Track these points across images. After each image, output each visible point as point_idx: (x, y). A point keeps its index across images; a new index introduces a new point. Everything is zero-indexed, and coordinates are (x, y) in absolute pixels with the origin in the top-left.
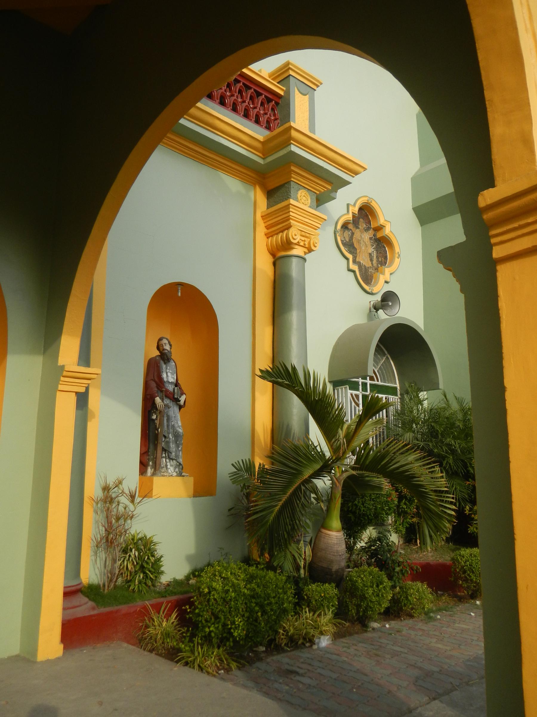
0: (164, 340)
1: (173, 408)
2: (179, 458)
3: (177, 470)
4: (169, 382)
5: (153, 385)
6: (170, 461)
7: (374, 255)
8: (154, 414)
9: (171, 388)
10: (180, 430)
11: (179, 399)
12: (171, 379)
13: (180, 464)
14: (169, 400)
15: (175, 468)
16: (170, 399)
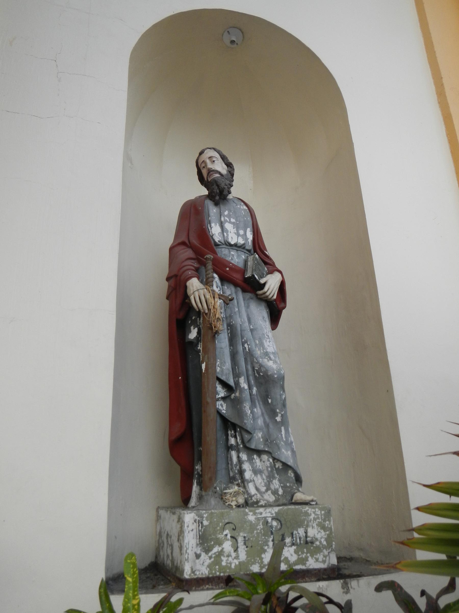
1: (248, 307)
2: (279, 449)
3: (276, 484)
4: (231, 245)
6: (250, 460)
8: (192, 328)
11: (258, 282)
12: (235, 237)
13: (286, 466)
14: (233, 288)
15: (270, 478)
16: (236, 285)
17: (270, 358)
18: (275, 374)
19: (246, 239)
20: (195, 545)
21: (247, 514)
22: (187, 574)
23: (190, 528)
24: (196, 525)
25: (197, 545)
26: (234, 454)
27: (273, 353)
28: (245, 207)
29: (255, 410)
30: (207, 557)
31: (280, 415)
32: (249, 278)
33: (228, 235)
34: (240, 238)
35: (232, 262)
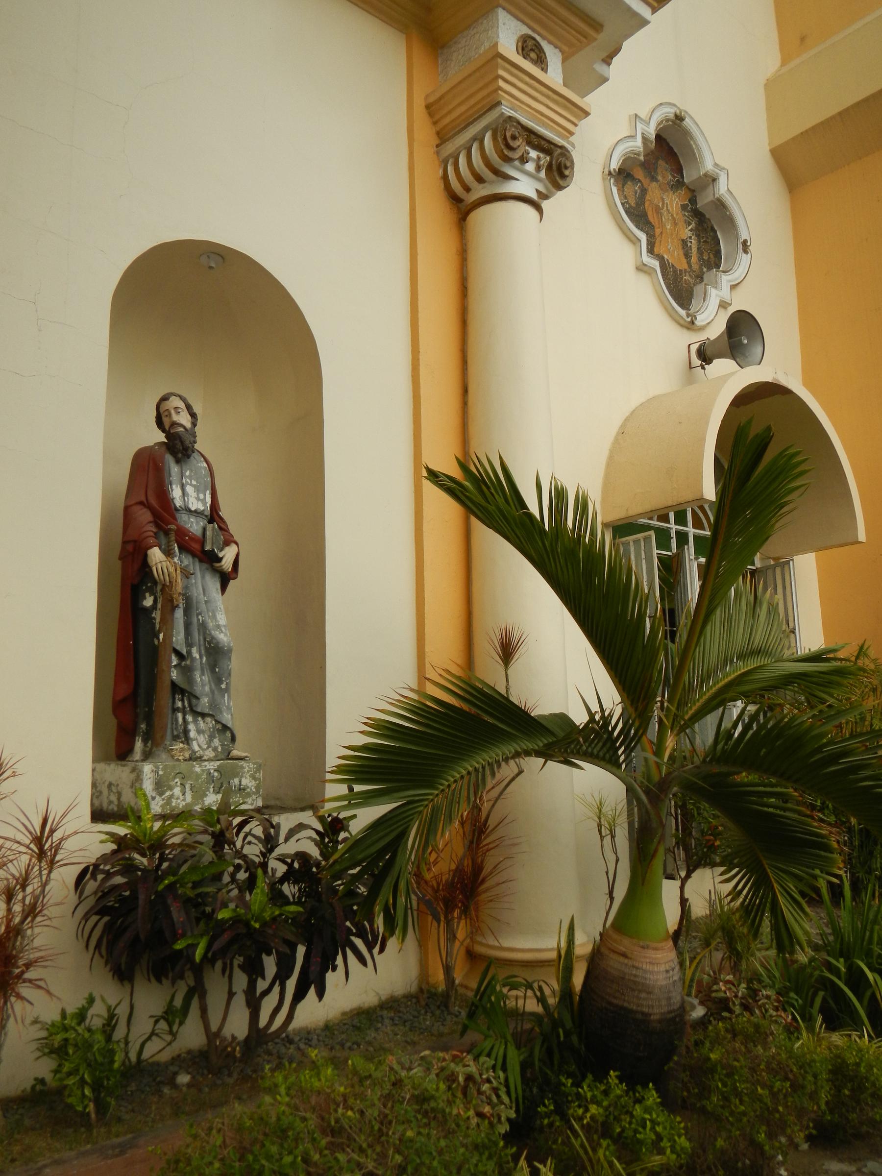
0: (173, 398)
1: (203, 577)
2: (221, 712)
3: (216, 742)
4: (190, 511)
5: (144, 516)
6: (195, 721)
7: (693, 246)
8: (147, 595)
9: (195, 526)
10: (223, 638)
11: (216, 556)
12: (195, 501)
13: (225, 728)
14: (191, 559)
15: (211, 738)
16: (194, 555)
17: (221, 630)
18: (225, 646)
19: (205, 503)
20: (151, 790)
21: (194, 766)
23: (148, 777)
24: (153, 774)
25: (153, 790)
26: (180, 716)
27: (224, 626)
28: (205, 465)
29: (204, 678)
30: (160, 799)
31: (225, 683)
32: (208, 551)
33: (188, 499)
34: (200, 502)
35: (191, 530)
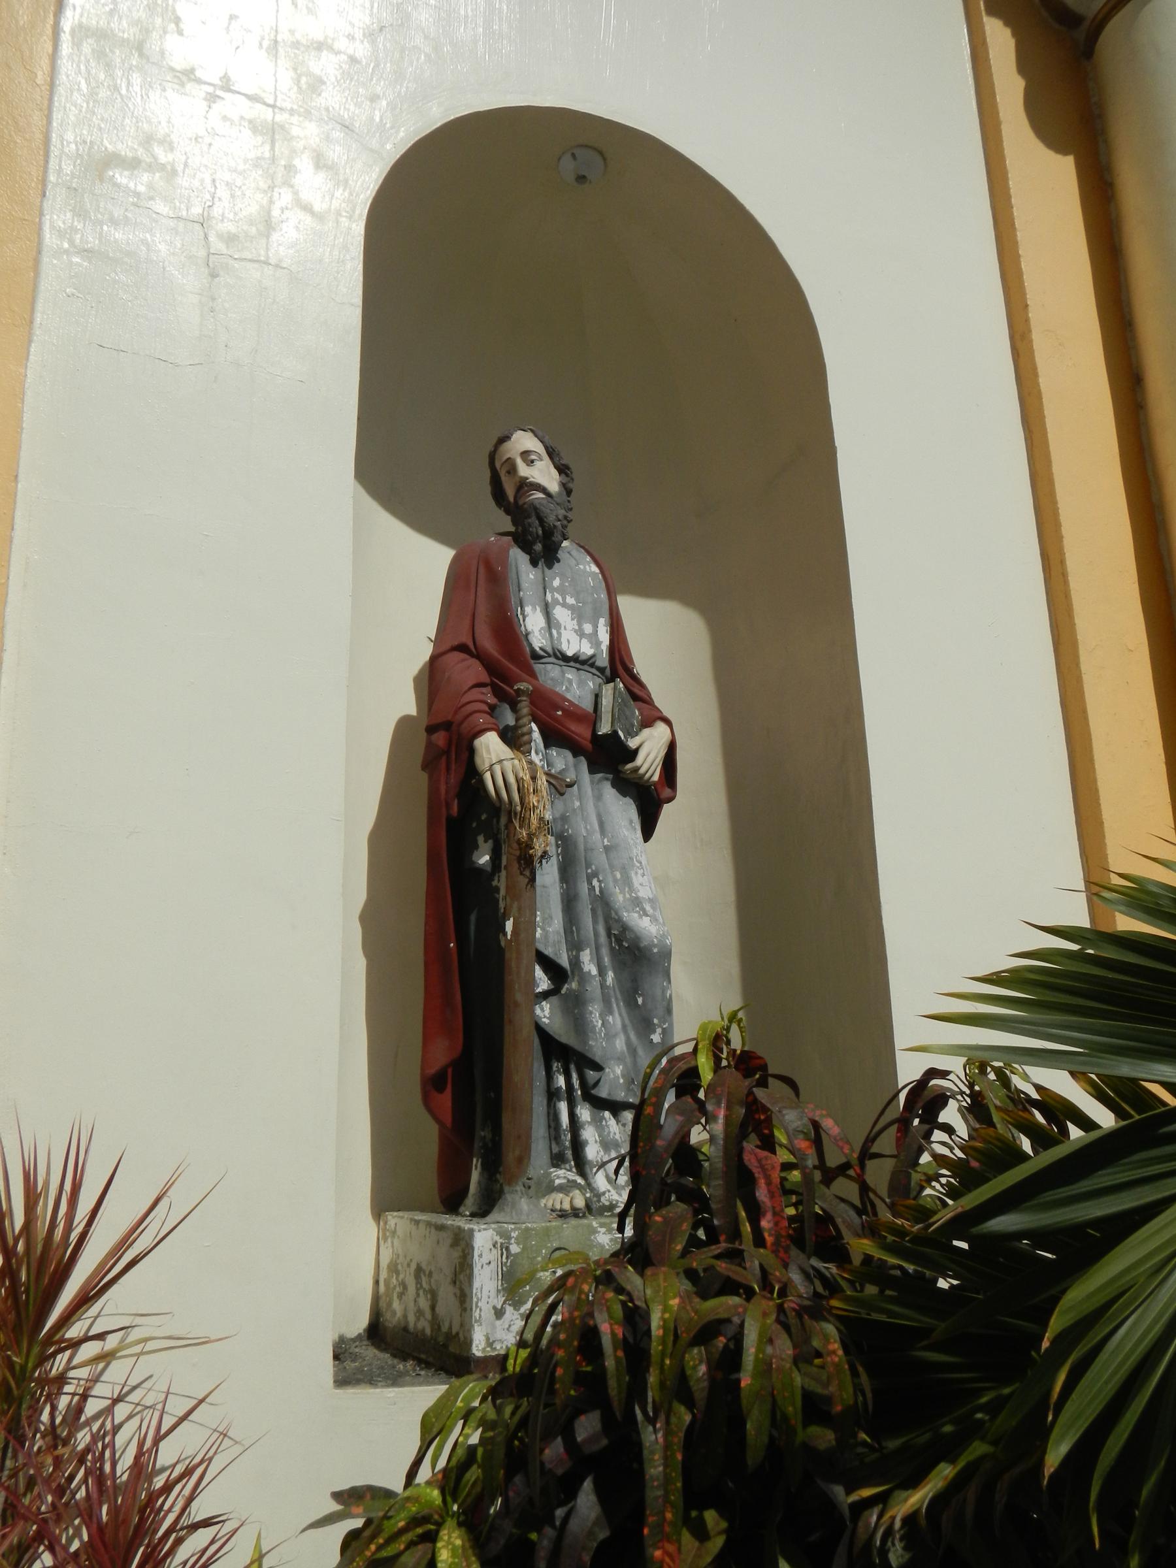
1: (598, 797)
4: (565, 659)
5: (469, 671)
6: (597, 1122)
8: (481, 839)
10: (646, 926)
12: (575, 639)
16: (577, 750)
17: (644, 910)
18: (655, 946)
19: (596, 644)
20: (493, 1293)
21: (595, 1231)
22: (478, 1348)
23: (485, 1260)
24: (496, 1253)
25: (498, 1291)
26: (563, 1107)
27: (650, 900)
28: (595, 569)
29: (610, 1019)
30: (516, 1315)
31: (659, 1030)
32: (605, 736)
33: (559, 634)
34: (584, 641)
35: (569, 696)
